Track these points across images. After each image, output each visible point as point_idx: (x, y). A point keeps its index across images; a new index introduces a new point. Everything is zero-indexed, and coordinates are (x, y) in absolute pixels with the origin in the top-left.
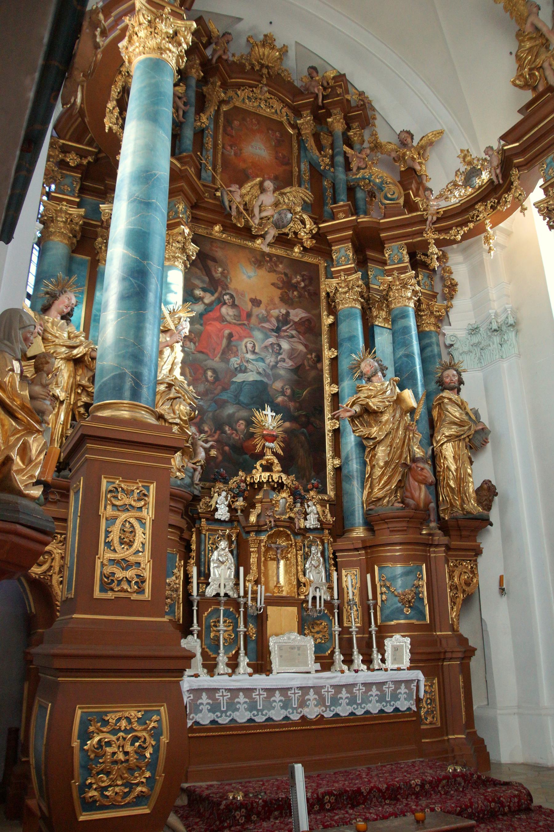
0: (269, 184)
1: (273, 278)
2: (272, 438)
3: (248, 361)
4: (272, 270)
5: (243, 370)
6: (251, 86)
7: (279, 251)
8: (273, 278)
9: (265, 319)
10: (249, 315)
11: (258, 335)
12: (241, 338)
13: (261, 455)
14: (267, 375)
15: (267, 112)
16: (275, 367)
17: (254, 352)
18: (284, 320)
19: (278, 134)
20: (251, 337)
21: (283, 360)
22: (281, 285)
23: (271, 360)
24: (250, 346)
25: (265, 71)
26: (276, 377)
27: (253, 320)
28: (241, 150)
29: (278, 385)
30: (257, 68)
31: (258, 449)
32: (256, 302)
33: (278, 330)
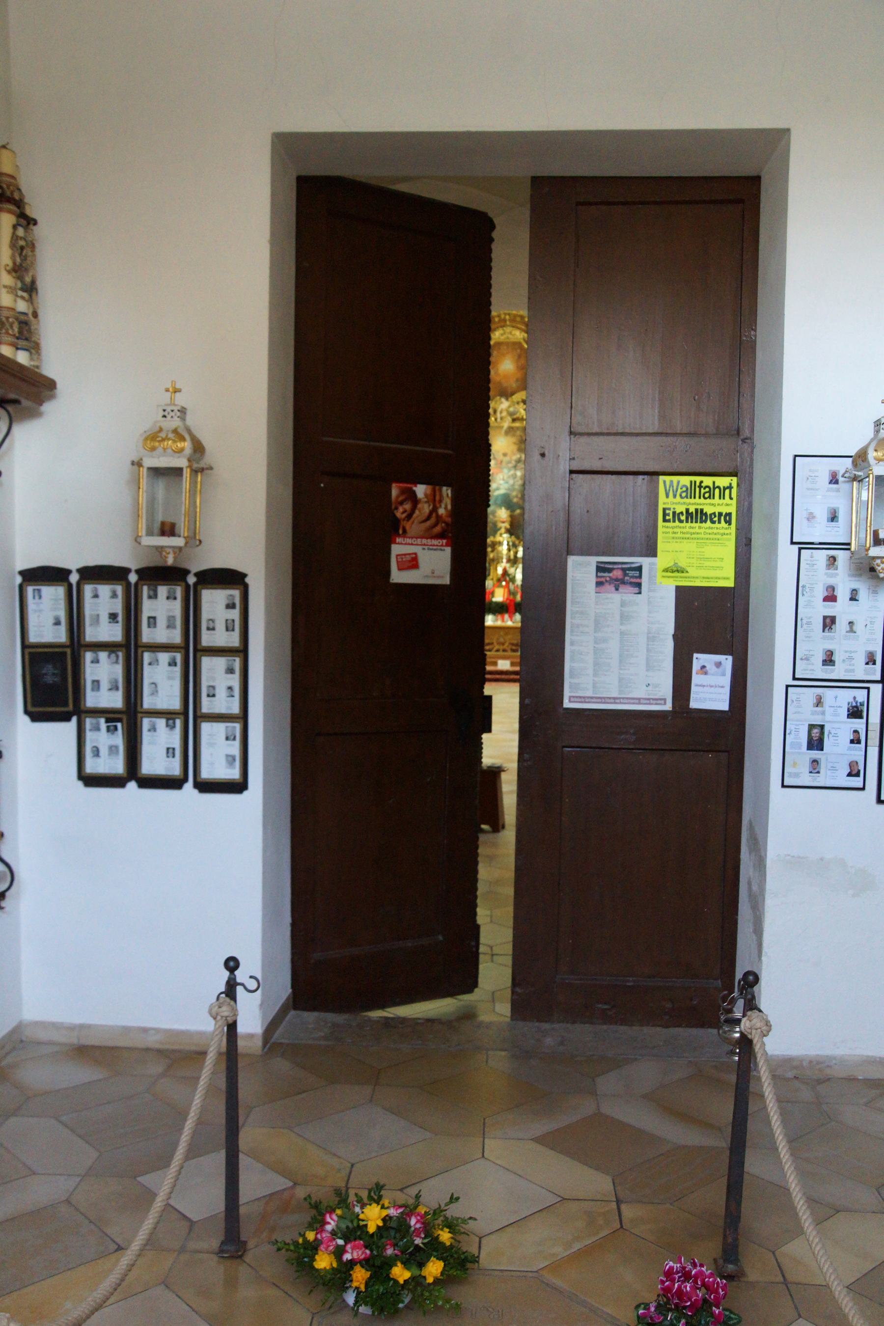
0: (503, 400)
1: (514, 440)
2: (503, 522)
3: (501, 484)
4: (514, 435)
5: (498, 489)
6: (502, 327)
7: (517, 424)
8: (514, 440)
9: (510, 462)
10: (501, 462)
11: (505, 471)
12: (497, 474)
13: (500, 528)
14: (509, 489)
15: (512, 339)
16: (513, 485)
17: (503, 479)
18: (519, 461)
19: (519, 351)
20: (502, 472)
21: (518, 481)
22: (518, 442)
23: (511, 482)
24: (501, 477)
25: (507, 317)
26: (514, 490)
27: (504, 464)
28: (498, 369)
29: (514, 494)
30: (503, 316)
31: (498, 527)
32: (505, 455)
33: (515, 467)
